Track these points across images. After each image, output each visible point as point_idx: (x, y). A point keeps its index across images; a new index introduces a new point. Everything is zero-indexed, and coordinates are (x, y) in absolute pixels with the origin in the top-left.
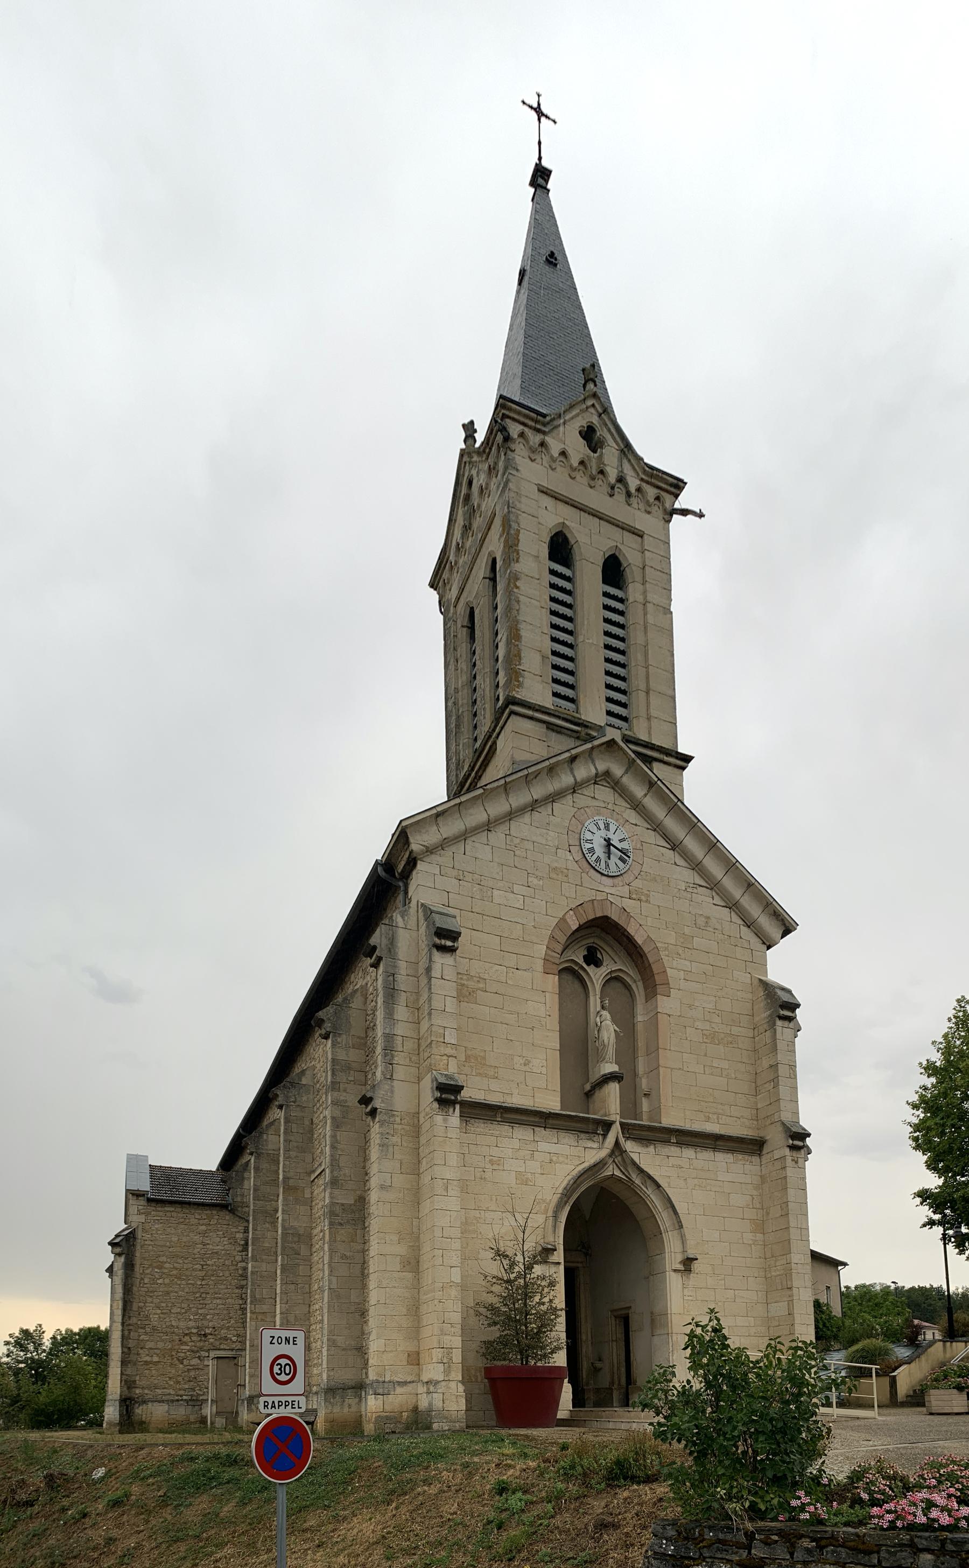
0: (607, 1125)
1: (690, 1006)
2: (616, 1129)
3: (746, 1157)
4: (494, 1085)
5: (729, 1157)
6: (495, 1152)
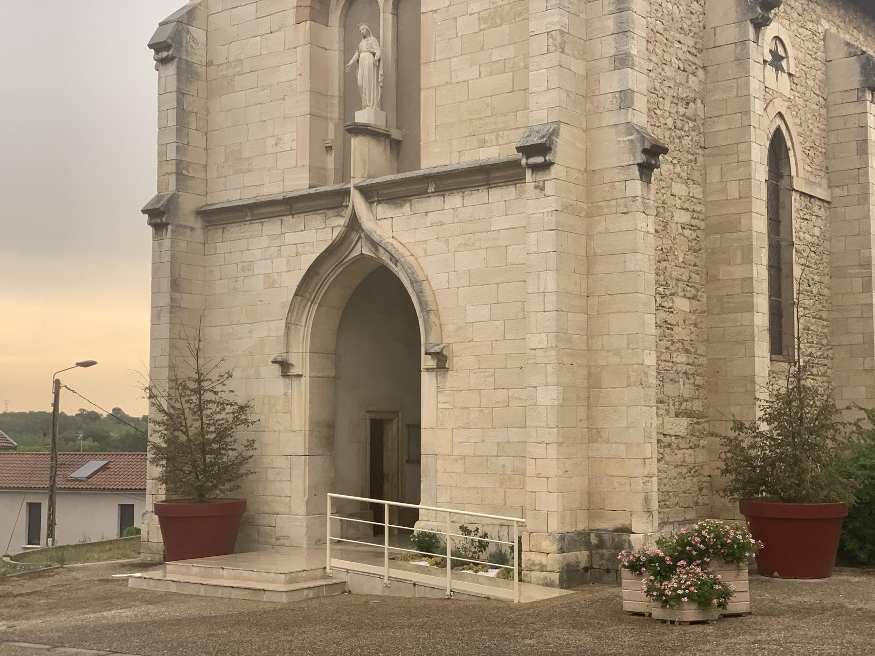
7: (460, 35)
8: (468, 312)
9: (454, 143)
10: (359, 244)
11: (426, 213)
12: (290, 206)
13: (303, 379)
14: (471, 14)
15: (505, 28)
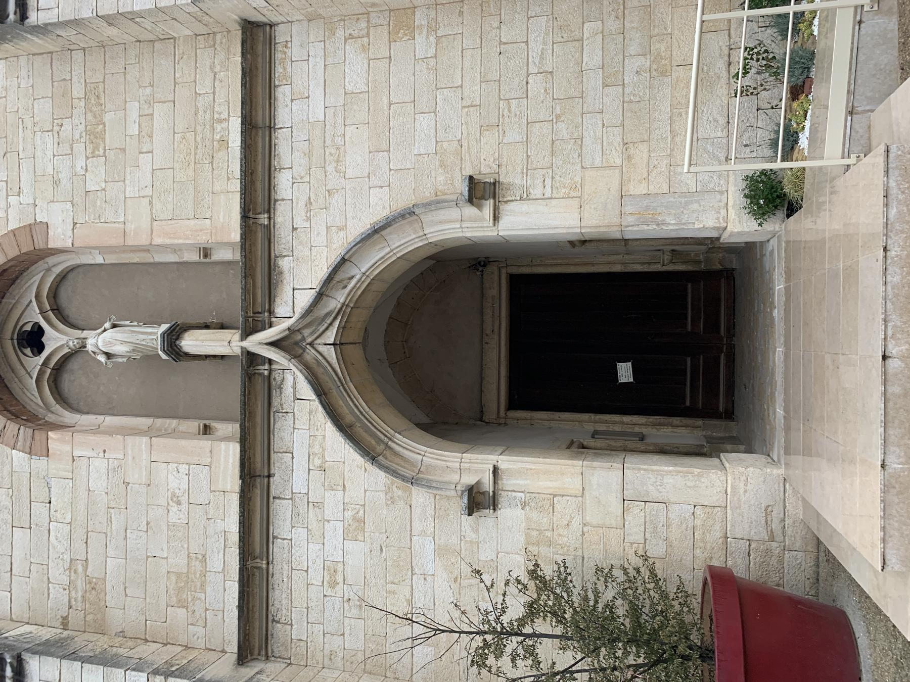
0: (251, 358)
1: (56, 183)
2: (256, 343)
3: (279, 56)
4: (215, 562)
5: (283, 94)
6: (316, 577)
7: (103, 185)
8: (423, 151)
9: (217, 188)
10: (321, 348)
11: (294, 229)
12: (255, 477)
13: (502, 466)
14: (86, 170)
15: (108, 117)
